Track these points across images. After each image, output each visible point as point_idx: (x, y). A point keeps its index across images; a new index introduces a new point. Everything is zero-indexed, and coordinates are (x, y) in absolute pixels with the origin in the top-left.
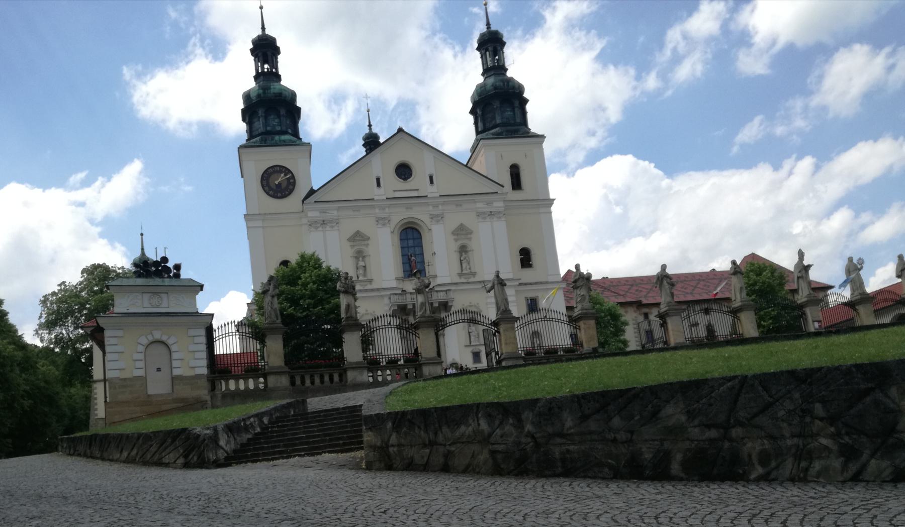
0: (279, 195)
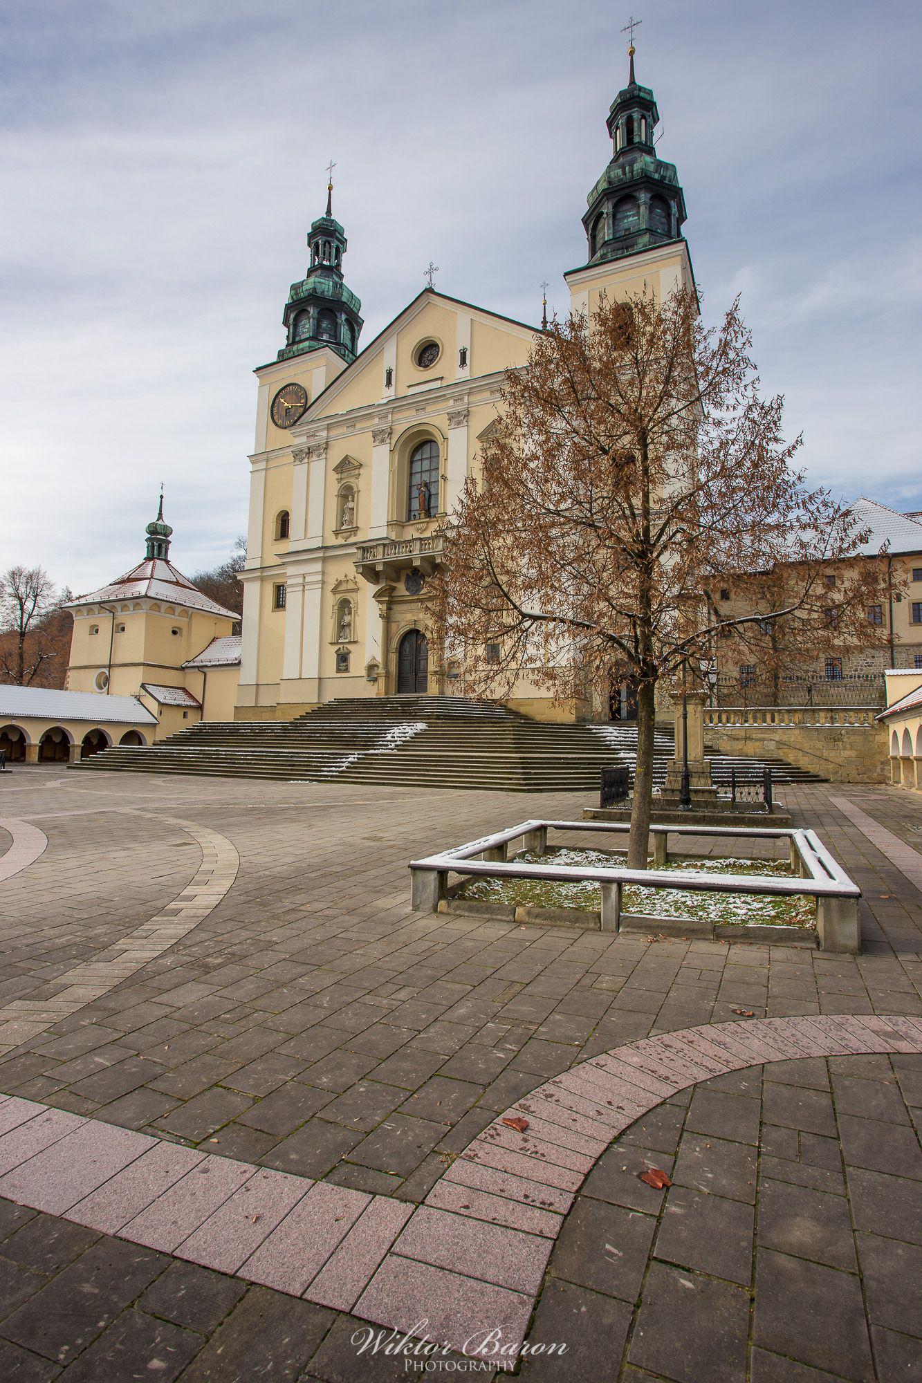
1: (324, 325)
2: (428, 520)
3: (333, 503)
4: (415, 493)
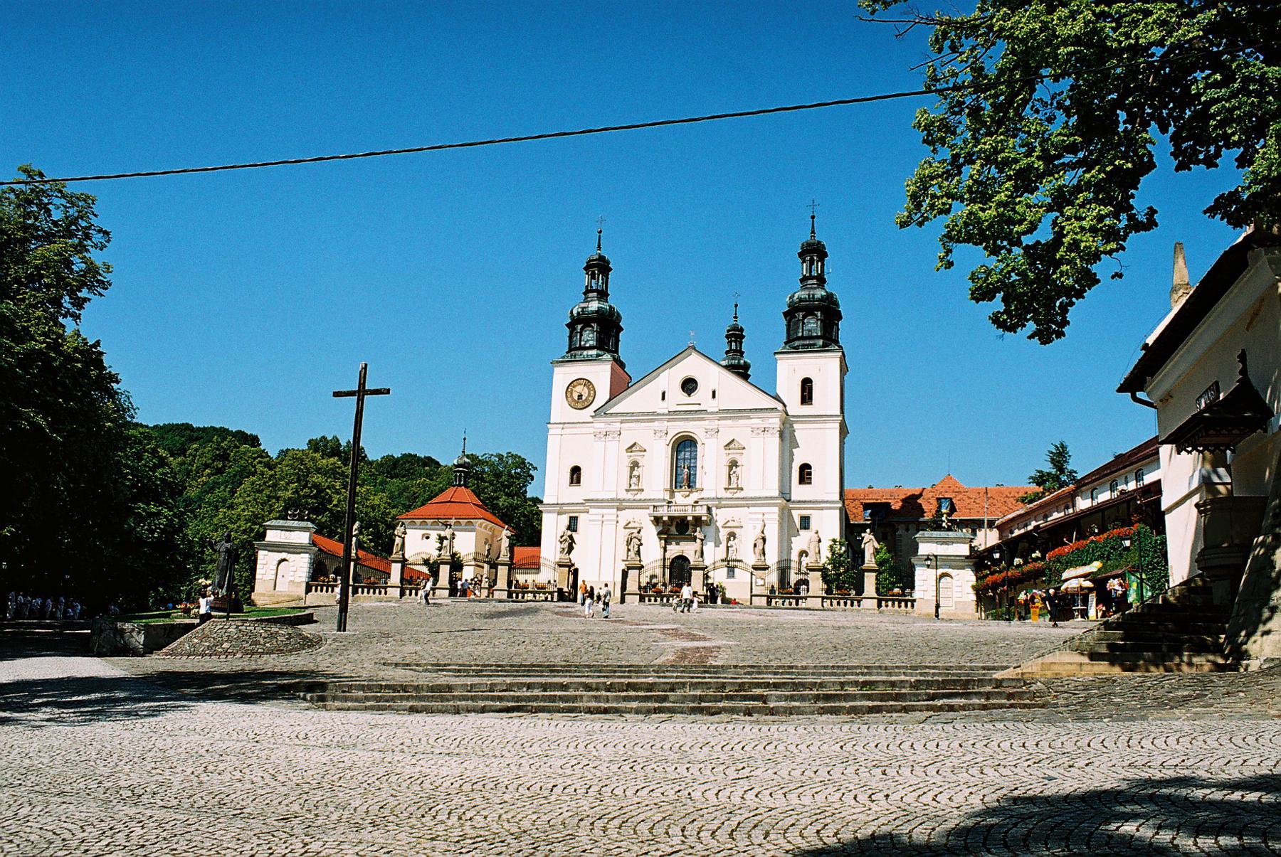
0: (580, 406)
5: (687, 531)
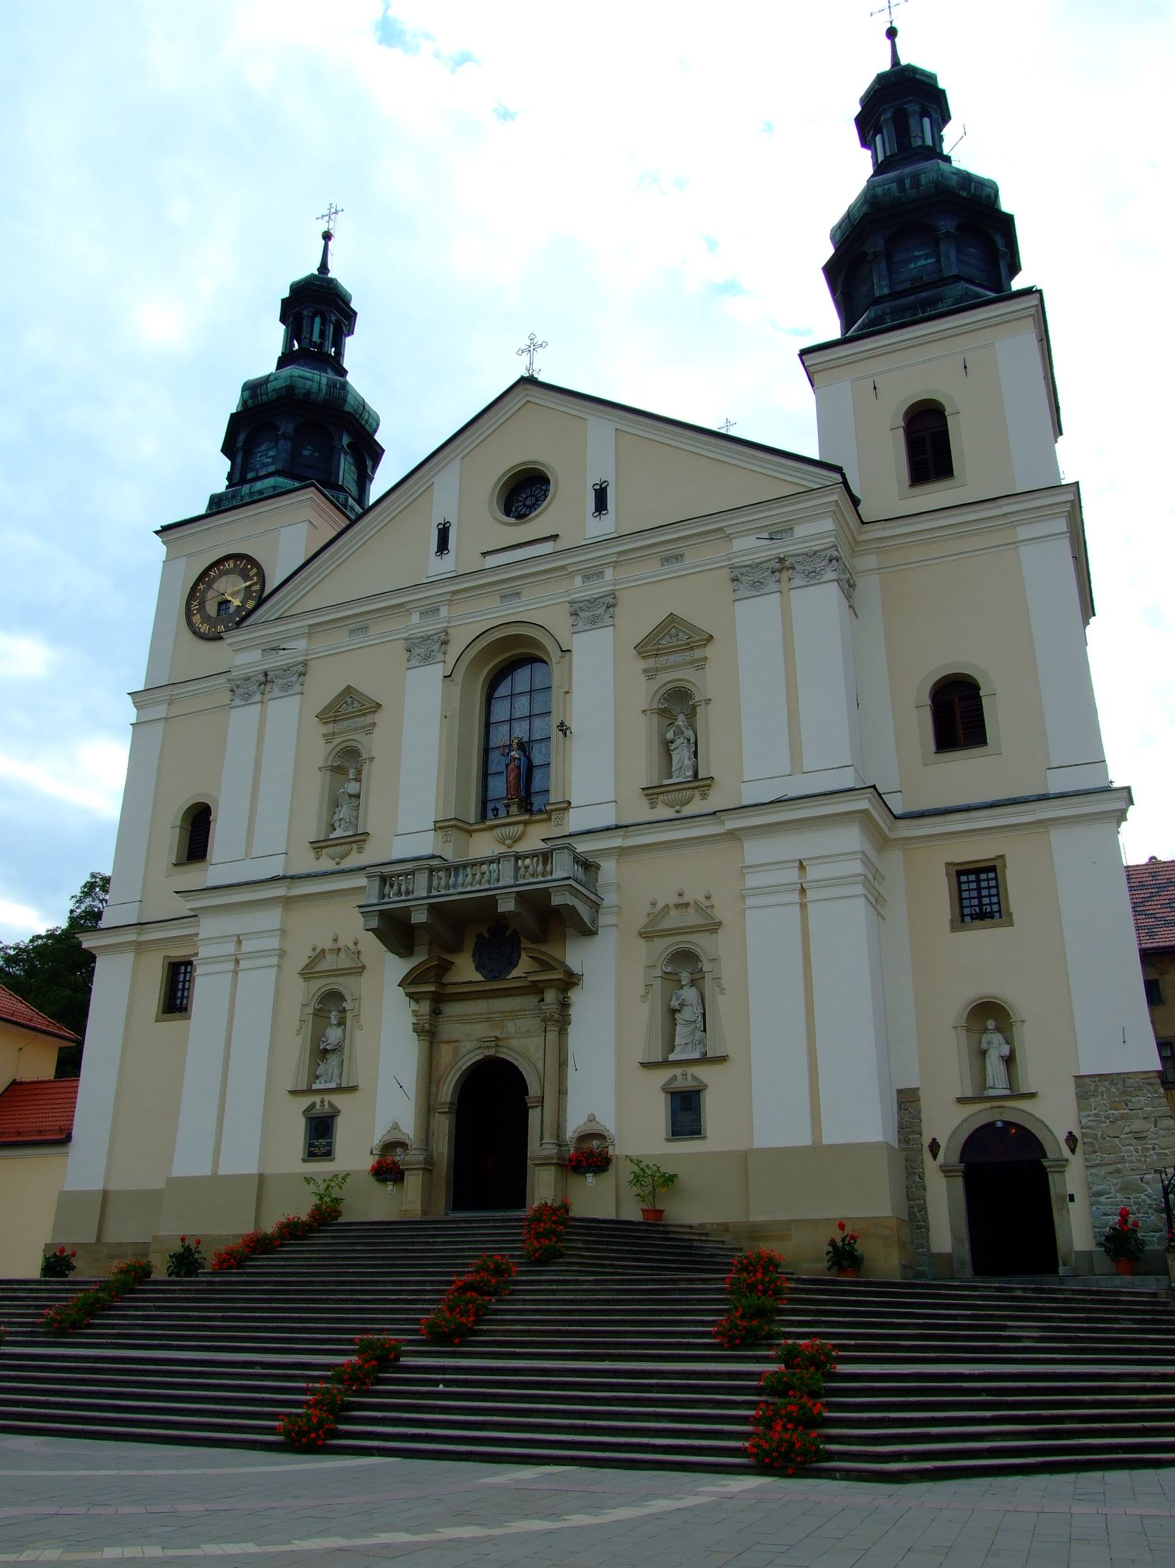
1: (306, 453)
2: (526, 817)
3: (316, 784)
4: (497, 762)
5: (514, 965)
